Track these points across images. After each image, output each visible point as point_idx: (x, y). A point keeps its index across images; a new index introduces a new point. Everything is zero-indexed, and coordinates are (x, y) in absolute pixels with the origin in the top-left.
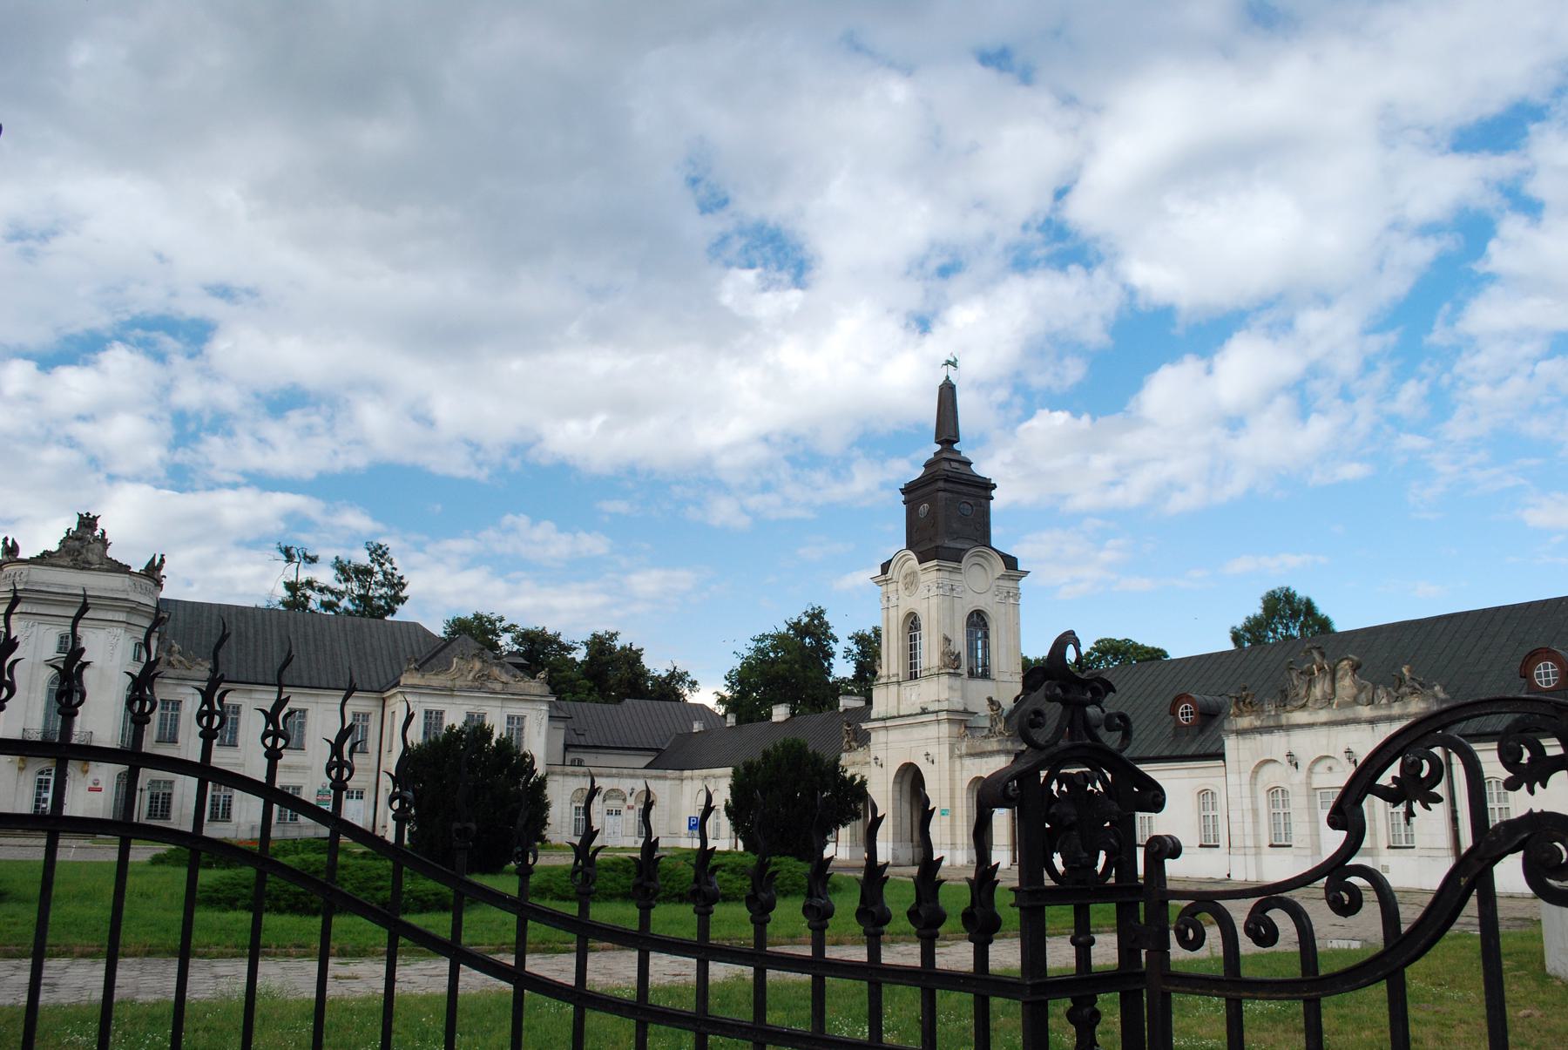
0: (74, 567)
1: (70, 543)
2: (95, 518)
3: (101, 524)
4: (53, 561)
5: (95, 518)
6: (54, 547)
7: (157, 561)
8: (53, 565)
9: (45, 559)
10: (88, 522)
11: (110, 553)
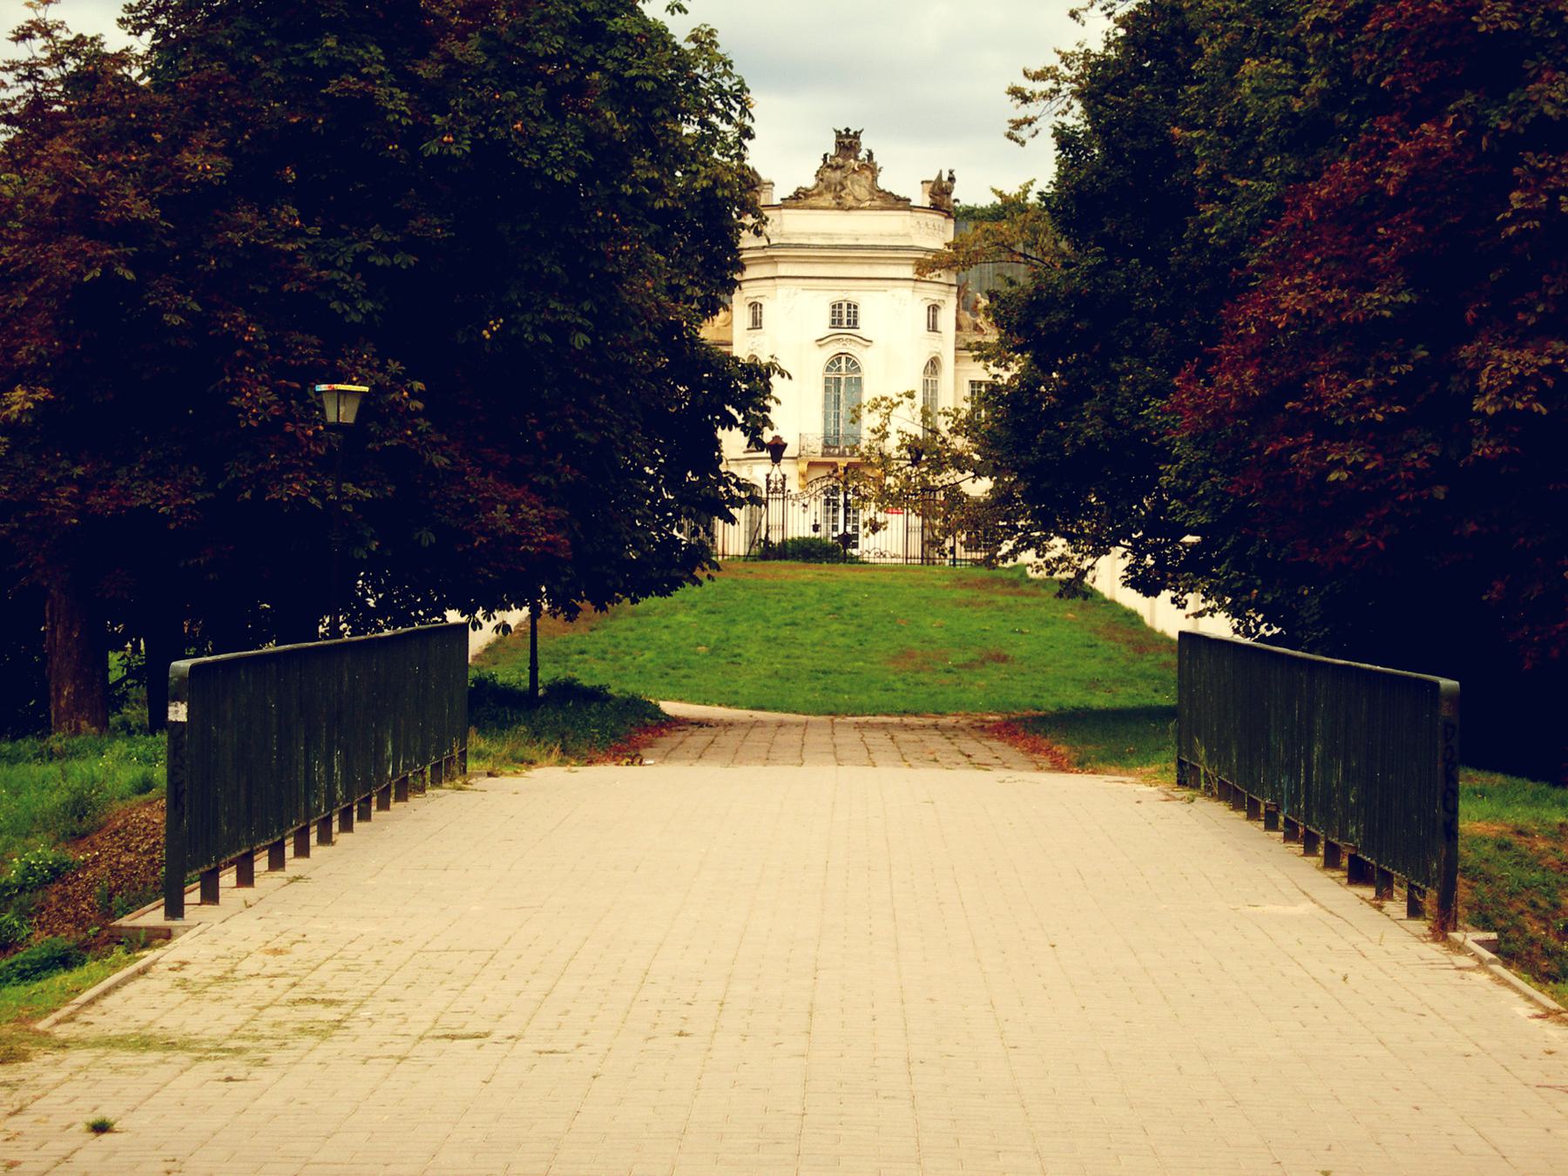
0: (840, 207)
1: (828, 173)
2: (857, 135)
3: (866, 143)
4: (811, 201)
5: (857, 135)
6: (809, 182)
7: (945, 178)
8: (812, 208)
9: (799, 199)
10: (847, 143)
11: (883, 183)
